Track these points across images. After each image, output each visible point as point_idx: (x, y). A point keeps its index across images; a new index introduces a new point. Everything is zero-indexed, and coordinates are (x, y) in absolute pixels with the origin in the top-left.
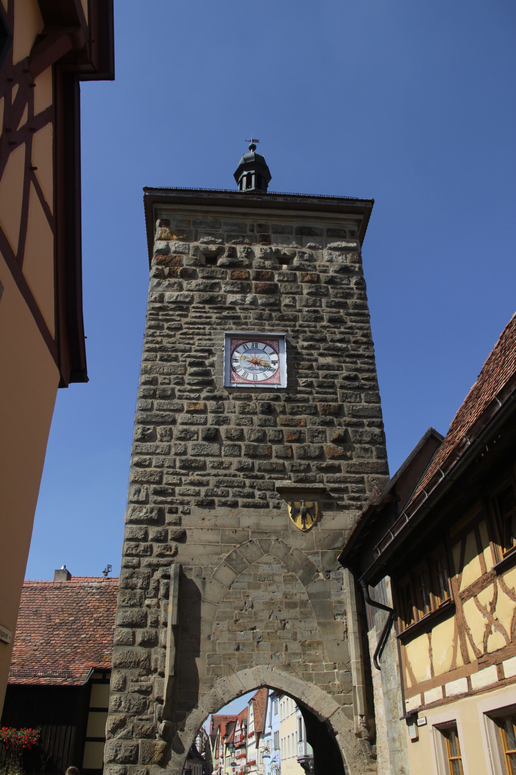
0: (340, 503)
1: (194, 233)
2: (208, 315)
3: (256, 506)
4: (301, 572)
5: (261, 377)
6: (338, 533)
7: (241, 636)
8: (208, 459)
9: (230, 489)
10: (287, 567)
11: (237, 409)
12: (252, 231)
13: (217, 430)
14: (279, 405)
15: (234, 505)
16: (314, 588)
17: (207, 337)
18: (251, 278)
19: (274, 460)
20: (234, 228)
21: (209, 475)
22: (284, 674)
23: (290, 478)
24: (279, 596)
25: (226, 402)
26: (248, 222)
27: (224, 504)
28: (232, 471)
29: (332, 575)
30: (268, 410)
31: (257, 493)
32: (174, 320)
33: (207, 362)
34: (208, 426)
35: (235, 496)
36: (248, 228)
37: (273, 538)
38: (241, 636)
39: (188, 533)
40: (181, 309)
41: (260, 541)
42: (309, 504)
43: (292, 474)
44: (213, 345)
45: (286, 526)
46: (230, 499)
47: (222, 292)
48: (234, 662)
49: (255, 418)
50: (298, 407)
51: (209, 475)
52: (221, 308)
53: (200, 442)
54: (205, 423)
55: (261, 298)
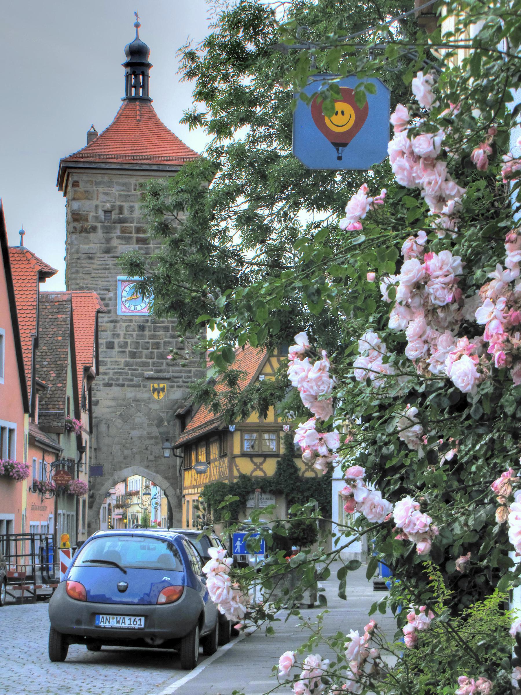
0: (178, 384)
1: (96, 192)
2: (108, 262)
3: (134, 386)
4: (156, 422)
5: (138, 308)
6: (176, 401)
7: (126, 452)
8: (109, 360)
9: (121, 377)
10: (149, 419)
11: (124, 329)
12: (135, 190)
13: (113, 342)
14: (149, 326)
15: (123, 385)
16: (162, 430)
17: (107, 279)
18: (133, 232)
19: (144, 360)
20: (123, 188)
21: (109, 369)
22: (146, 470)
23: (152, 370)
24: (145, 433)
25: (118, 325)
26: (133, 181)
27: (118, 385)
28: (122, 366)
29: (171, 423)
30: (142, 328)
31: (136, 379)
32: (86, 267)
33: (107, 297)
34: (109, 340)
35: (123, 380)
36: (132, 187)
37: (143, 404)
38: (126, 452)
39: (100, 401)
40: (90, 258)
41: (136, 405)
42: (161, 386)
43: (154, 368)
44: (111, 285)
45: (149, 397)
46: (121, 382)
47: (115, 245)
48: (123, 466)
49: (135, 334)
50: (160, 327)
51: (109, 369)
52: (114, 257)
53: (105, 349)
54: (107, 338)
55: (140, 249)
